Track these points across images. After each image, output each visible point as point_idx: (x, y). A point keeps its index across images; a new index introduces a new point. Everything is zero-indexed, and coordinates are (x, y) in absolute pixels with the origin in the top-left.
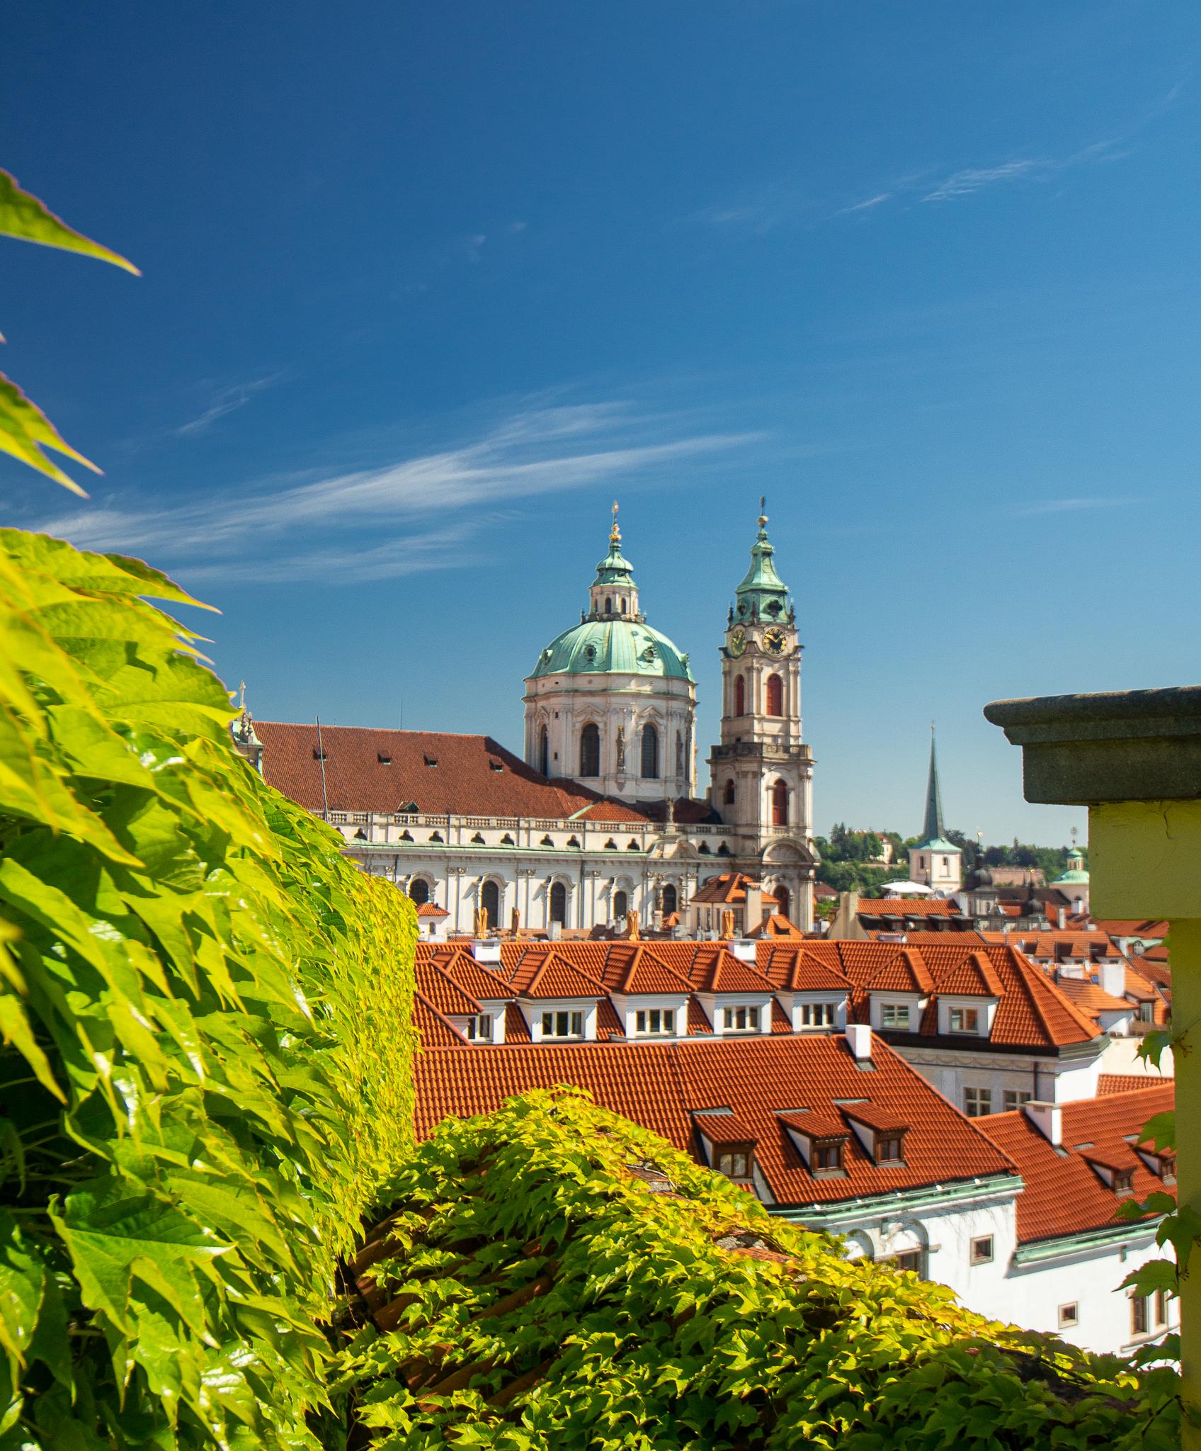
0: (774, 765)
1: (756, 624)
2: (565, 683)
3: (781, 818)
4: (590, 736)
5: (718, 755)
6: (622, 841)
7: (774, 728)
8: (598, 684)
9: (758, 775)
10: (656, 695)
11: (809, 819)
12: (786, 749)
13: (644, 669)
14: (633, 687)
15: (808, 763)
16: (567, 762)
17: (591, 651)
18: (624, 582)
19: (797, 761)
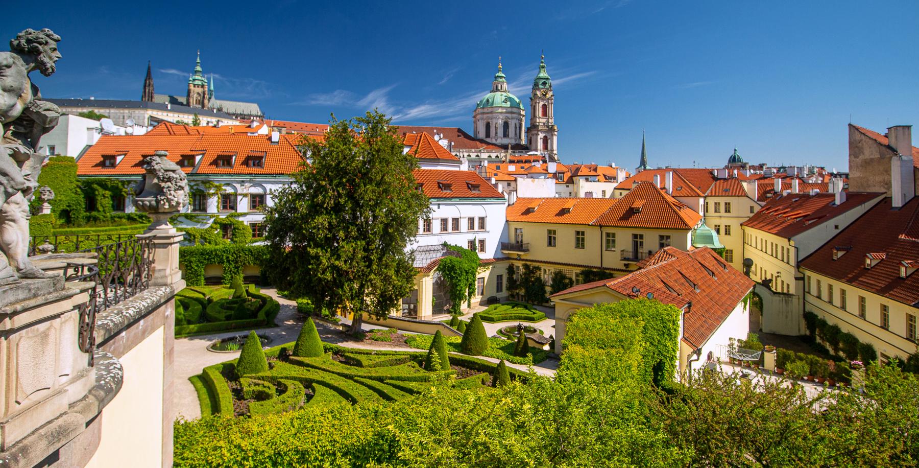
0: (542, 131)
1: (539, 89)
2: (481, 111)
3: (546, 147)
4: (488, 126)
5: (528, 130)
6: (493, 156)
7: (544, 120)
8: (490, 110)
9: (538, 134)
10: (506, 113)
11: (555, 147)
12: (548, 126)
13: (504, 105)
14: (500, 110)
15: (554, 131)
16: (482, 135)
17: (488, 101)
18: (501, 80)
19: (551, 130)
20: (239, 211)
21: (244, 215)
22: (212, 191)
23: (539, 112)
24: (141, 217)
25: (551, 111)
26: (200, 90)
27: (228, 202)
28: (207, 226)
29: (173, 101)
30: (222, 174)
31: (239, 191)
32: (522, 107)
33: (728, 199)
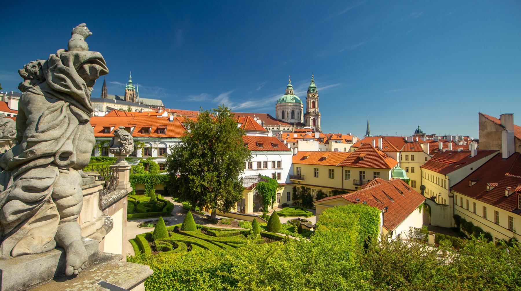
0: (312, 116)
1: (311, 93)
3: (314, 124)
4: (283, 113)
5: (305, 115)
6: (286, 129)
7: (314, 110)
8: (284, 104)
12: (315, 113)
16: (280, 117)
18: (290, 88)
19: (317, 115)
20: (153, 156)
21: (156, 158)
22: (139, 146)
23: (311, 105)
24: (103, 159)
25: (317, 105)
26: (131, 92)
27: (148, 152)
28: (137, 164)
29: (117, 98)
30: (144, 137)
31: (153, 146)
32: (301, 102)
33: (413, 153)
